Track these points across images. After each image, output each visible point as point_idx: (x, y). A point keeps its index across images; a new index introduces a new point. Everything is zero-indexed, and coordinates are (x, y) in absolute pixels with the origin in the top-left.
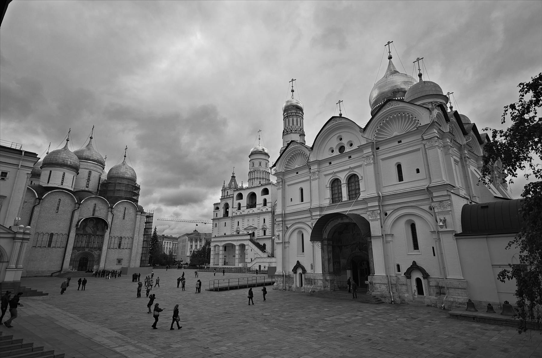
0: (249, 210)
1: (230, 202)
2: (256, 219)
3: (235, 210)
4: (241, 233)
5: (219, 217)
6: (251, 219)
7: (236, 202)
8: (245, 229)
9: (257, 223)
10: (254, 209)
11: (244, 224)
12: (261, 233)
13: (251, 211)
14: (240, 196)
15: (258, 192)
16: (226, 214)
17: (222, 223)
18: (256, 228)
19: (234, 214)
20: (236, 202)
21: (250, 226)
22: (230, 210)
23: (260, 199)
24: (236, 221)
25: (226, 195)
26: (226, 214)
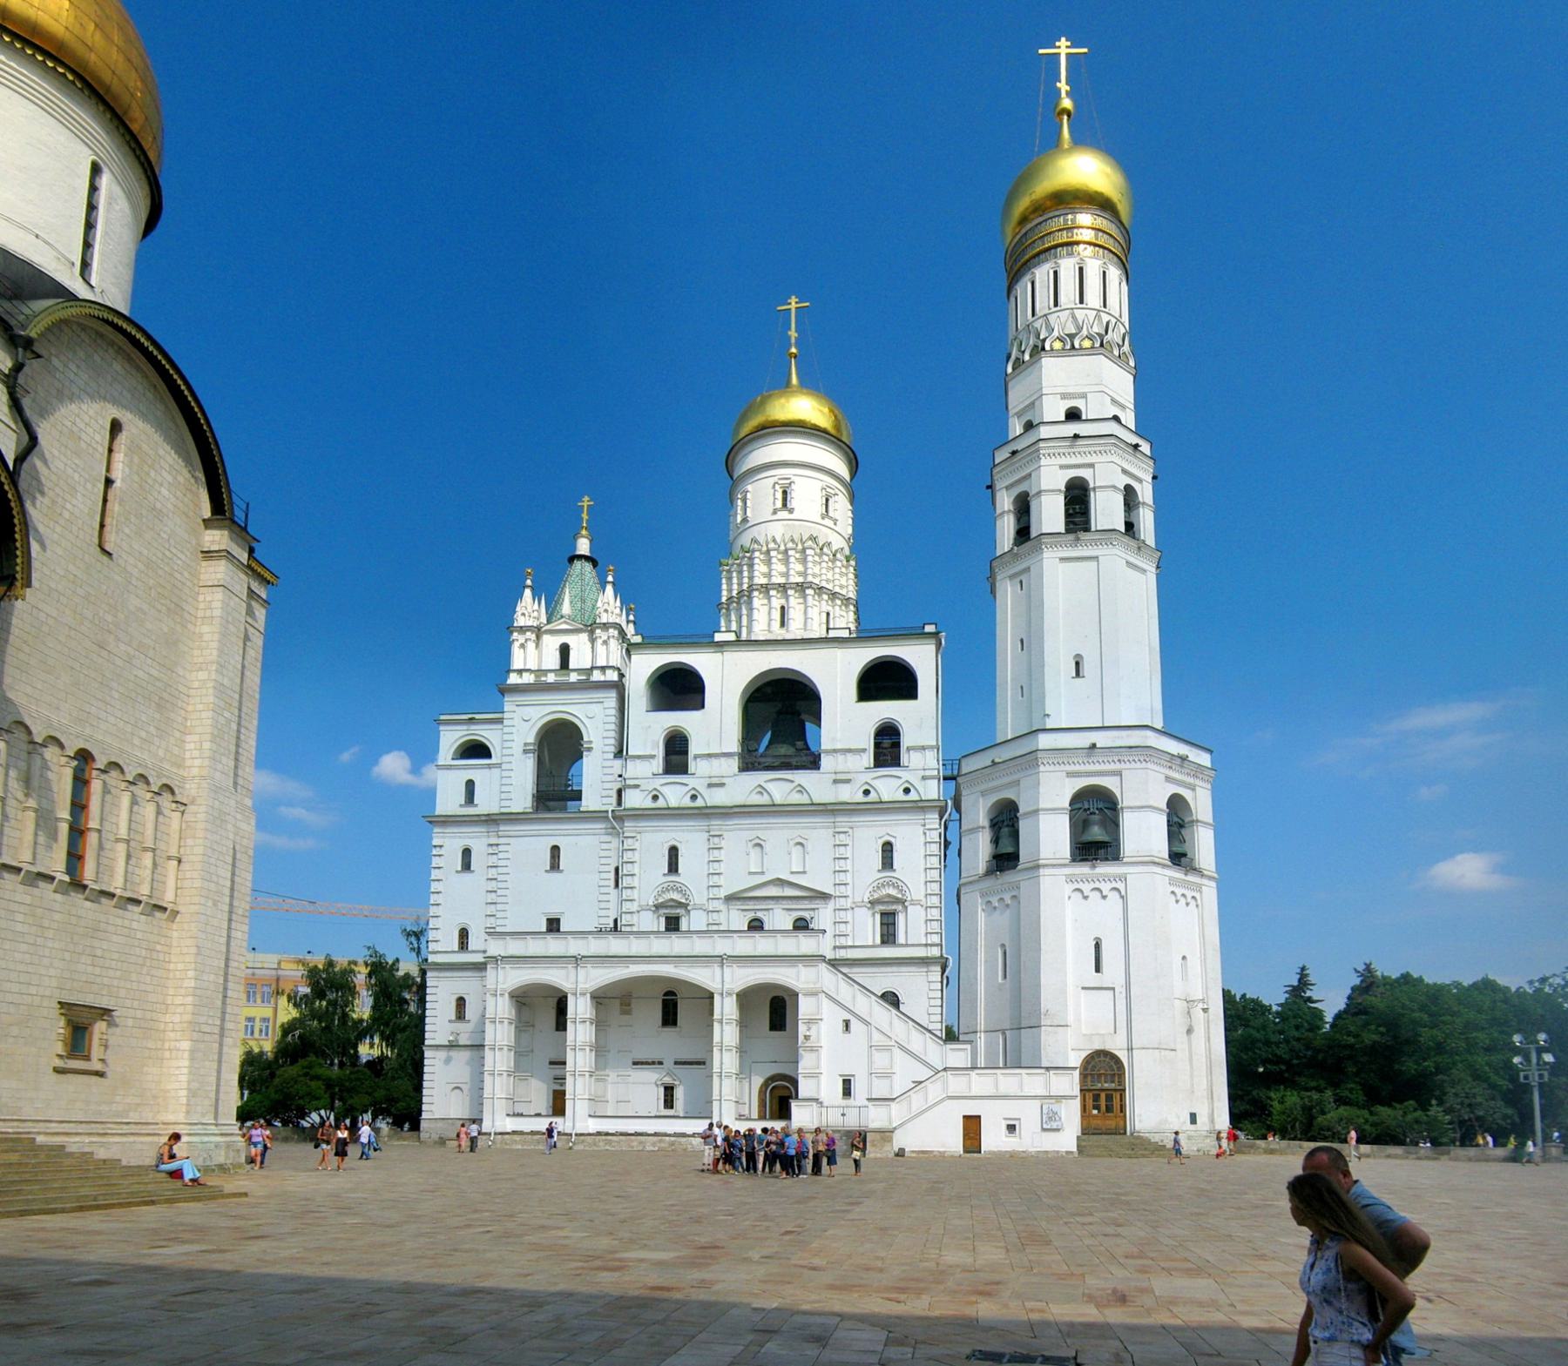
0: (761, 777)
1: (593, 718)
2: (818, 834)
3: (635, 770)
4: (693, 921)
5: (486, 803)
6: (778, 834)
7: (650, 728)
8: (731, 899)
9: (838, 862)
10: (802, 777)
11: (722, 864)
12: (867, 928)
13: (780, 787)
14: (680, 688)
15: (835, 674)
16: (555, 792)
17: (531, 844)
18: (824, 897)
19: (633, 800)
20: (650, 728)
21: (780, 882)
22: (595, 778)
23: (846, 722)
24: (651, 843)
25: (553, 661)
26: (555, 792)
